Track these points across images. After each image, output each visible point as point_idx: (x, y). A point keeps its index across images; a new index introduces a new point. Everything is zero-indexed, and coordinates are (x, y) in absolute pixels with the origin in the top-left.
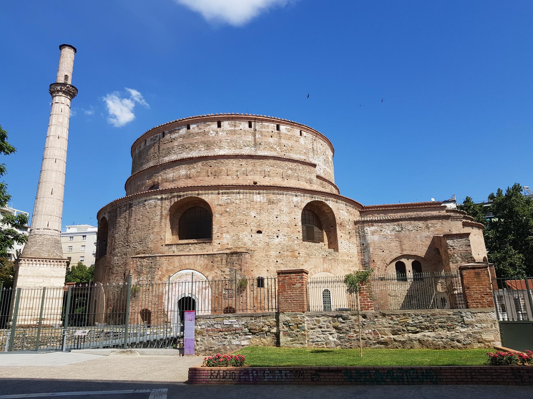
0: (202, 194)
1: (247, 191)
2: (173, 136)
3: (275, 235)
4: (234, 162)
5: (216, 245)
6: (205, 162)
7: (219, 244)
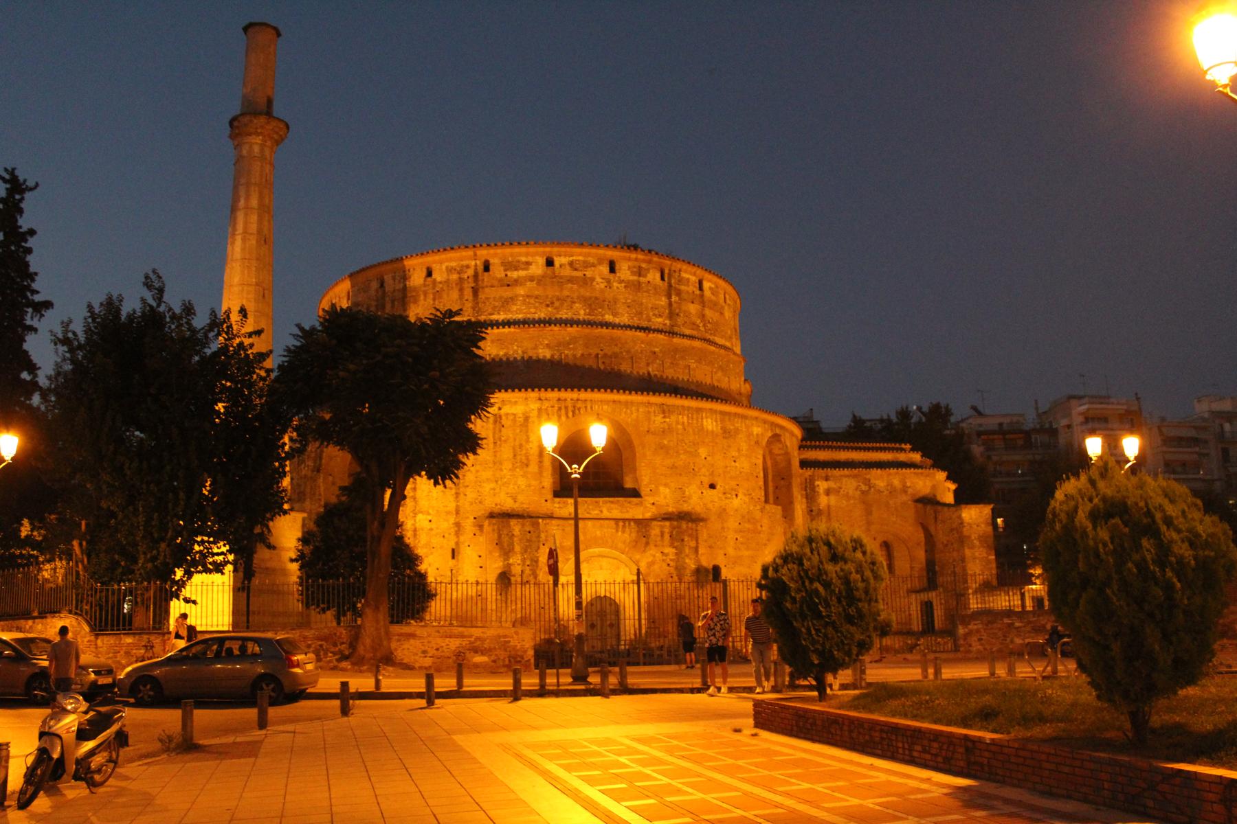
2: (514, 275)
3: (734, 493)
4: (643, 346)
5: (649, 505)
7: (653, 504)
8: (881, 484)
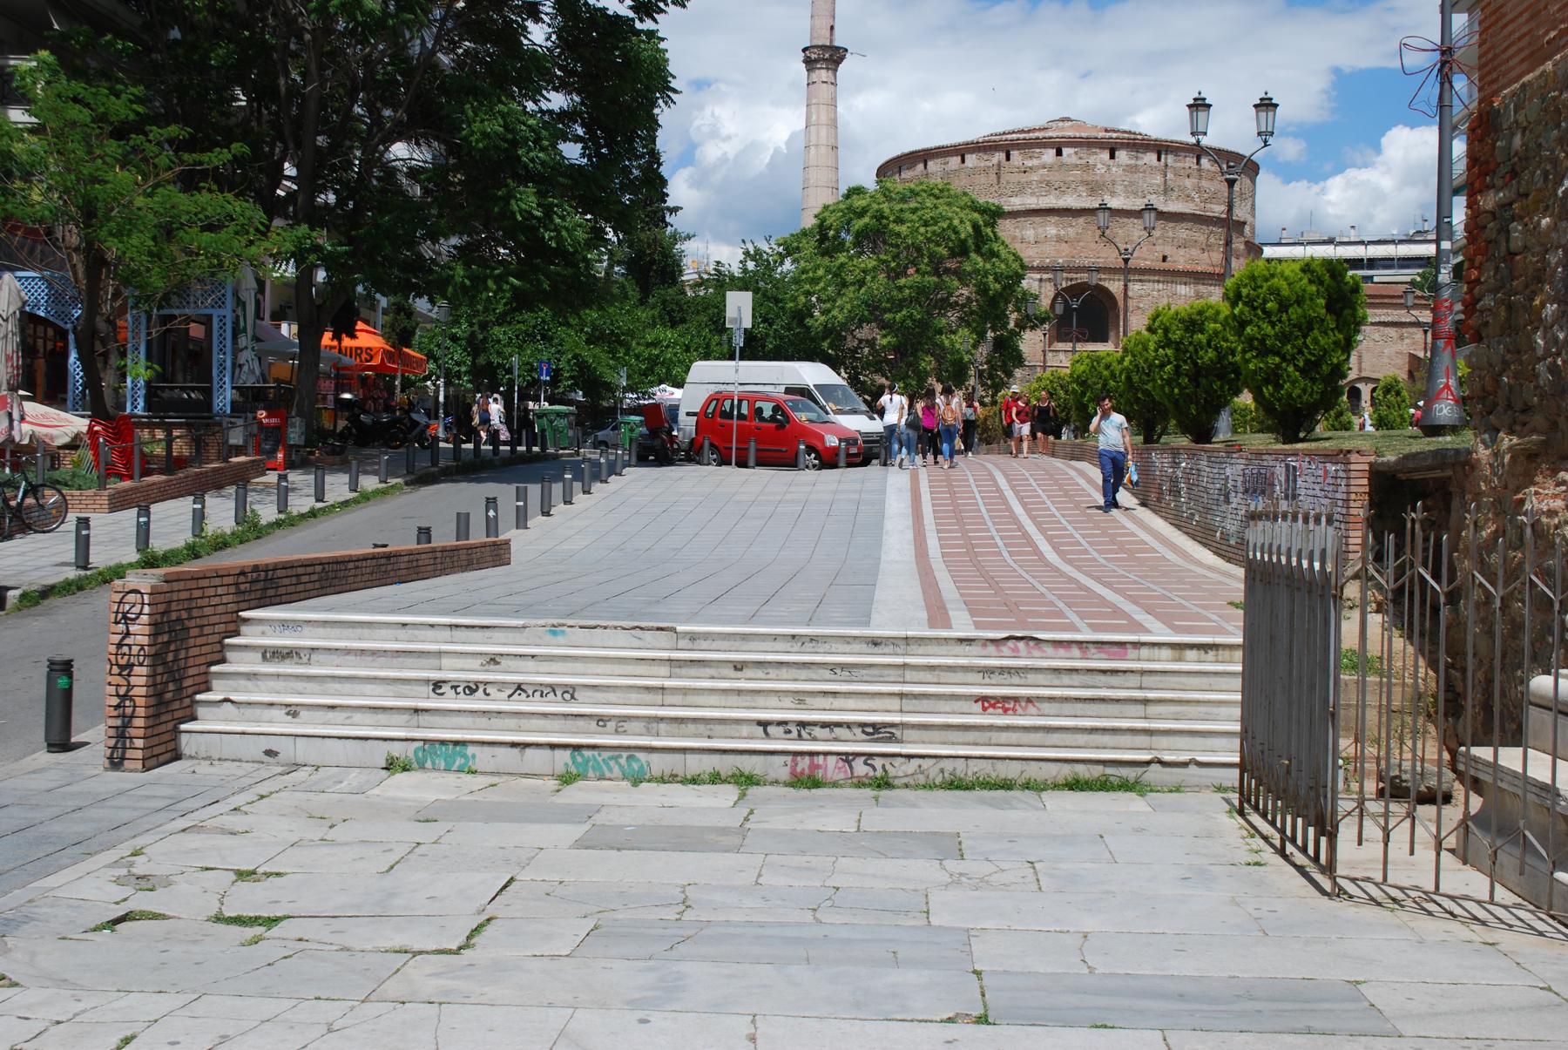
0: (1105, 280)
1: (1169, 279)
6: (1090, 219)
8: (1376, 336)
